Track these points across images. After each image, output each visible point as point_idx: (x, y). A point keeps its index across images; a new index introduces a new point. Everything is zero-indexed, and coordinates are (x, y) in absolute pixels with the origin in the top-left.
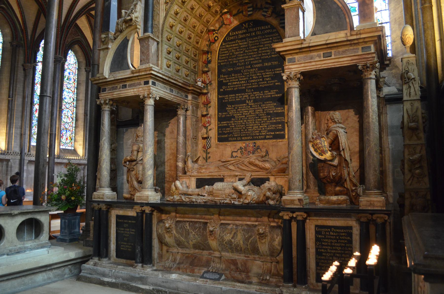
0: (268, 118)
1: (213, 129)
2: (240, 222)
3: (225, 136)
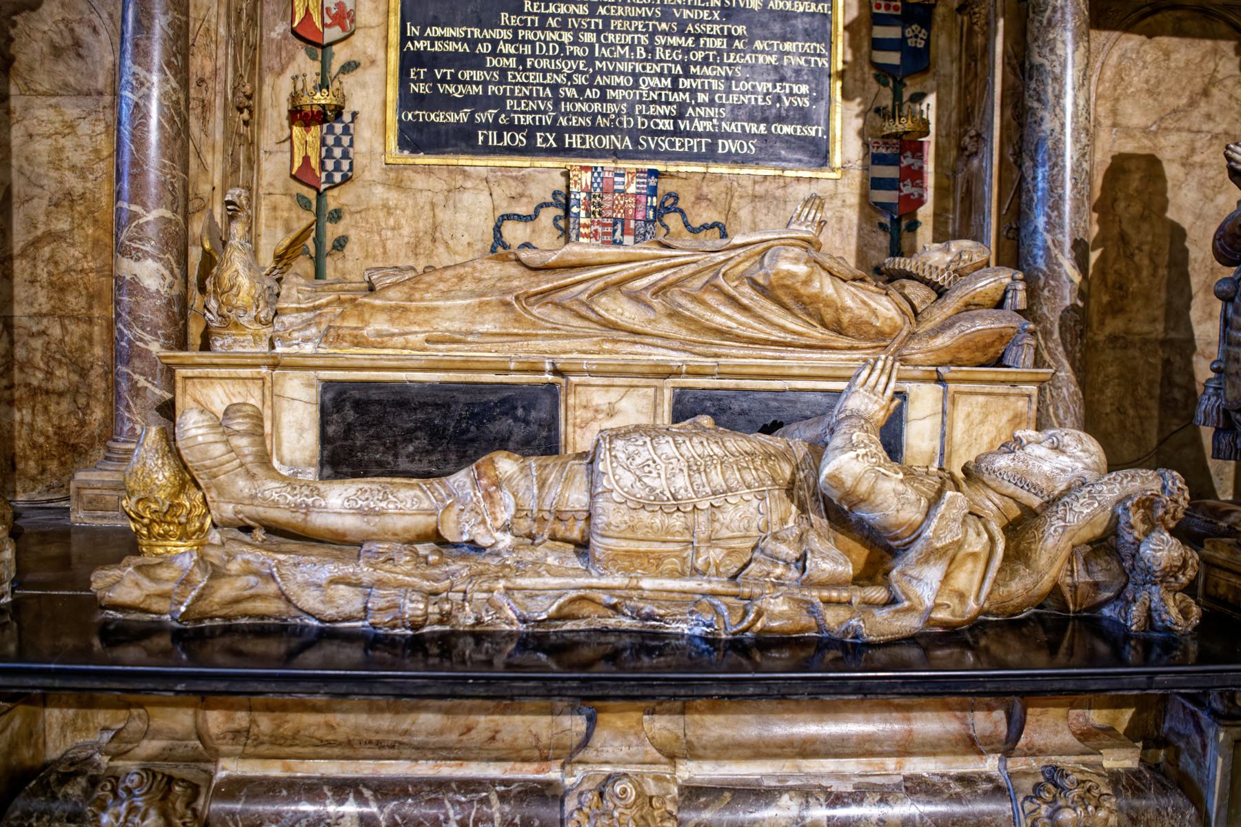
0: (731, 38)
1: (373, 62)
2: (851, 766)
3: (453, 118)
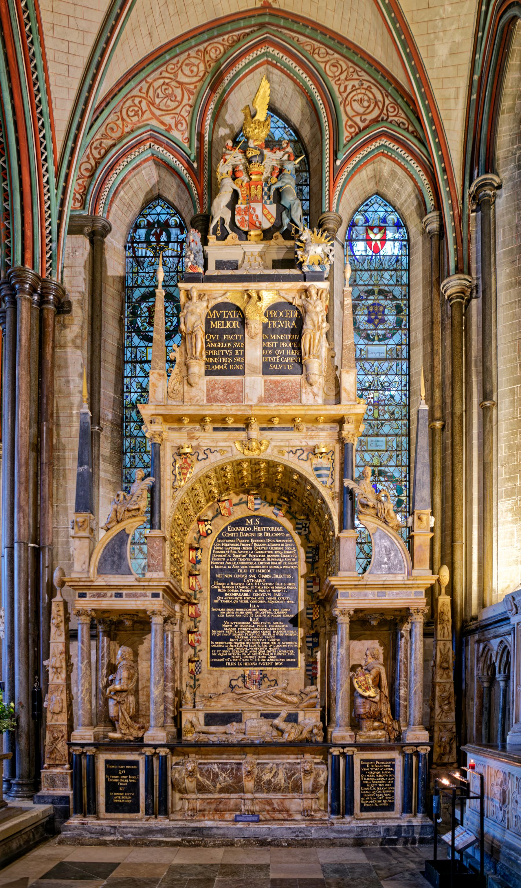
2: (280, 761)
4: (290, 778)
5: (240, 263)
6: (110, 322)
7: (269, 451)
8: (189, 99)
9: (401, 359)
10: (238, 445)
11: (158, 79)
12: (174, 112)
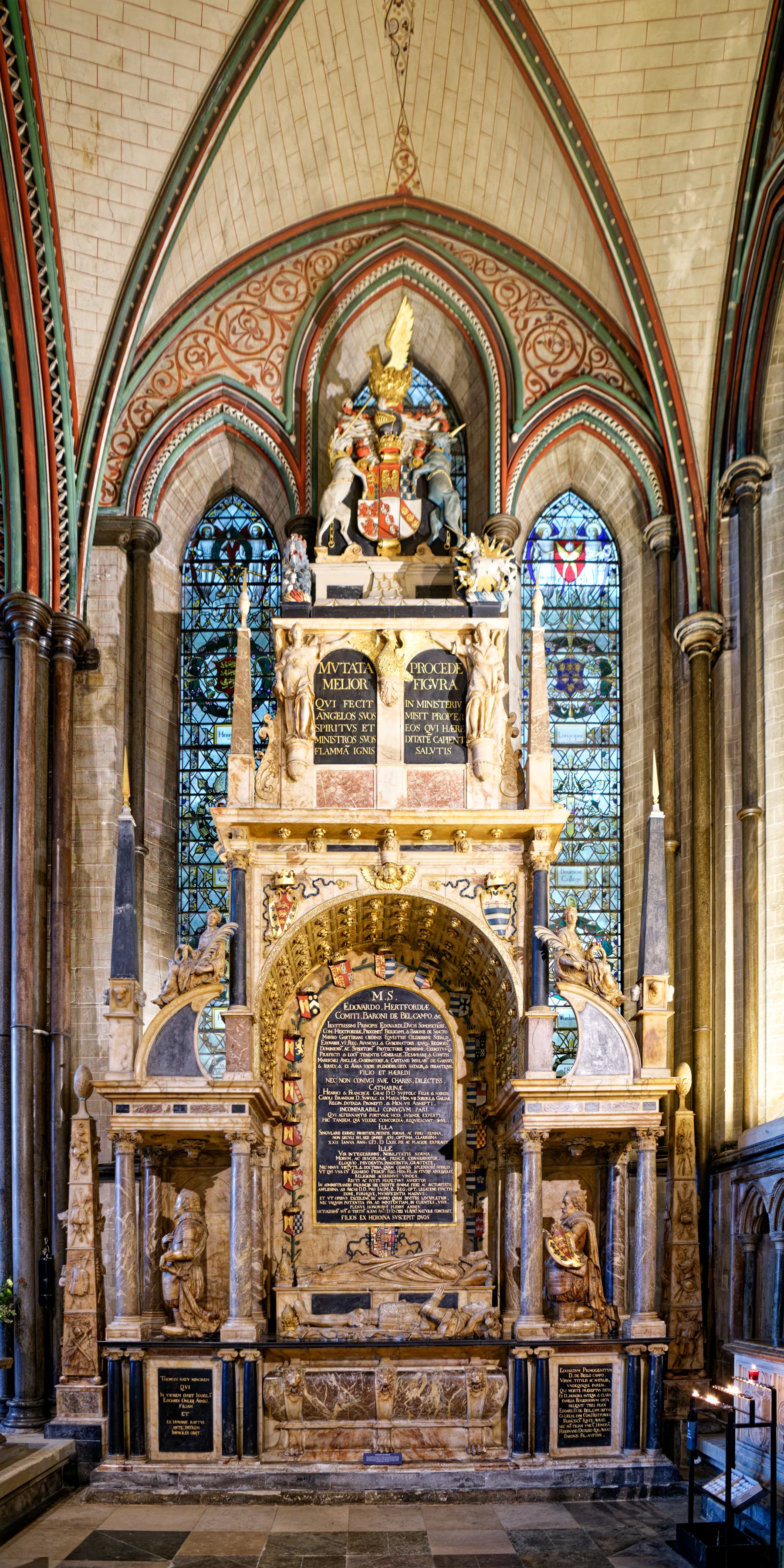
2: (433, 1368)
4: (449, 1395)
5: (365, 590)
6: (159, 684)
7: (415, 882)
8: (283, 337)
9: (609, 746)
10: (367, 872)
11: (234, 304)
12: (259, 356)
